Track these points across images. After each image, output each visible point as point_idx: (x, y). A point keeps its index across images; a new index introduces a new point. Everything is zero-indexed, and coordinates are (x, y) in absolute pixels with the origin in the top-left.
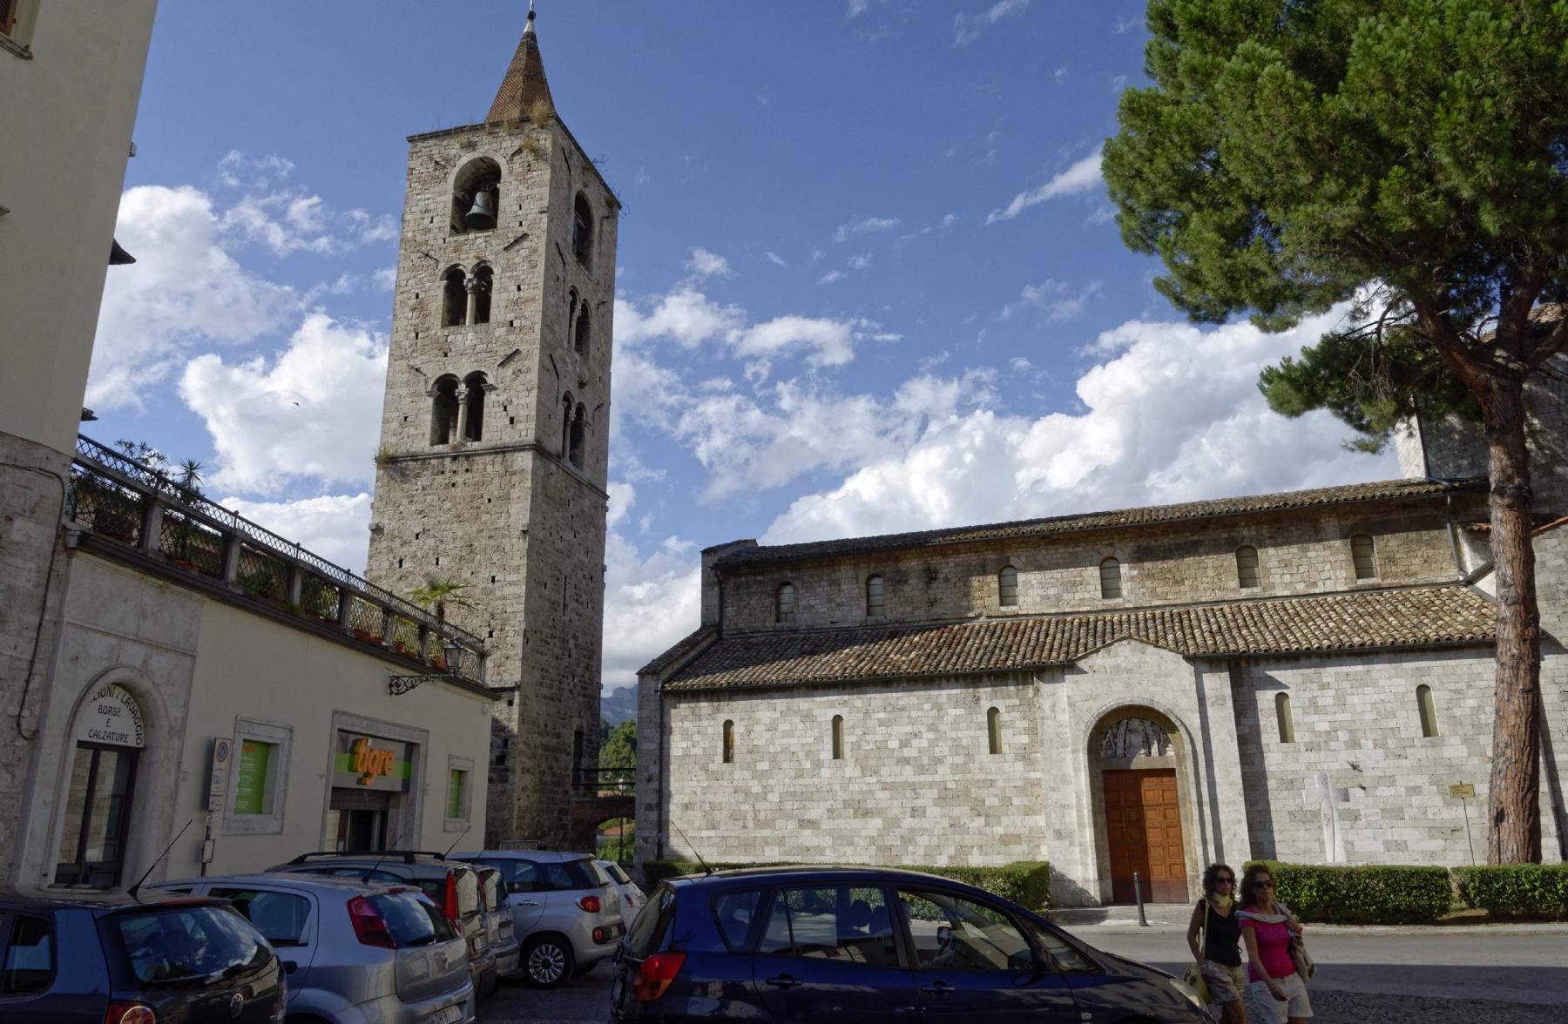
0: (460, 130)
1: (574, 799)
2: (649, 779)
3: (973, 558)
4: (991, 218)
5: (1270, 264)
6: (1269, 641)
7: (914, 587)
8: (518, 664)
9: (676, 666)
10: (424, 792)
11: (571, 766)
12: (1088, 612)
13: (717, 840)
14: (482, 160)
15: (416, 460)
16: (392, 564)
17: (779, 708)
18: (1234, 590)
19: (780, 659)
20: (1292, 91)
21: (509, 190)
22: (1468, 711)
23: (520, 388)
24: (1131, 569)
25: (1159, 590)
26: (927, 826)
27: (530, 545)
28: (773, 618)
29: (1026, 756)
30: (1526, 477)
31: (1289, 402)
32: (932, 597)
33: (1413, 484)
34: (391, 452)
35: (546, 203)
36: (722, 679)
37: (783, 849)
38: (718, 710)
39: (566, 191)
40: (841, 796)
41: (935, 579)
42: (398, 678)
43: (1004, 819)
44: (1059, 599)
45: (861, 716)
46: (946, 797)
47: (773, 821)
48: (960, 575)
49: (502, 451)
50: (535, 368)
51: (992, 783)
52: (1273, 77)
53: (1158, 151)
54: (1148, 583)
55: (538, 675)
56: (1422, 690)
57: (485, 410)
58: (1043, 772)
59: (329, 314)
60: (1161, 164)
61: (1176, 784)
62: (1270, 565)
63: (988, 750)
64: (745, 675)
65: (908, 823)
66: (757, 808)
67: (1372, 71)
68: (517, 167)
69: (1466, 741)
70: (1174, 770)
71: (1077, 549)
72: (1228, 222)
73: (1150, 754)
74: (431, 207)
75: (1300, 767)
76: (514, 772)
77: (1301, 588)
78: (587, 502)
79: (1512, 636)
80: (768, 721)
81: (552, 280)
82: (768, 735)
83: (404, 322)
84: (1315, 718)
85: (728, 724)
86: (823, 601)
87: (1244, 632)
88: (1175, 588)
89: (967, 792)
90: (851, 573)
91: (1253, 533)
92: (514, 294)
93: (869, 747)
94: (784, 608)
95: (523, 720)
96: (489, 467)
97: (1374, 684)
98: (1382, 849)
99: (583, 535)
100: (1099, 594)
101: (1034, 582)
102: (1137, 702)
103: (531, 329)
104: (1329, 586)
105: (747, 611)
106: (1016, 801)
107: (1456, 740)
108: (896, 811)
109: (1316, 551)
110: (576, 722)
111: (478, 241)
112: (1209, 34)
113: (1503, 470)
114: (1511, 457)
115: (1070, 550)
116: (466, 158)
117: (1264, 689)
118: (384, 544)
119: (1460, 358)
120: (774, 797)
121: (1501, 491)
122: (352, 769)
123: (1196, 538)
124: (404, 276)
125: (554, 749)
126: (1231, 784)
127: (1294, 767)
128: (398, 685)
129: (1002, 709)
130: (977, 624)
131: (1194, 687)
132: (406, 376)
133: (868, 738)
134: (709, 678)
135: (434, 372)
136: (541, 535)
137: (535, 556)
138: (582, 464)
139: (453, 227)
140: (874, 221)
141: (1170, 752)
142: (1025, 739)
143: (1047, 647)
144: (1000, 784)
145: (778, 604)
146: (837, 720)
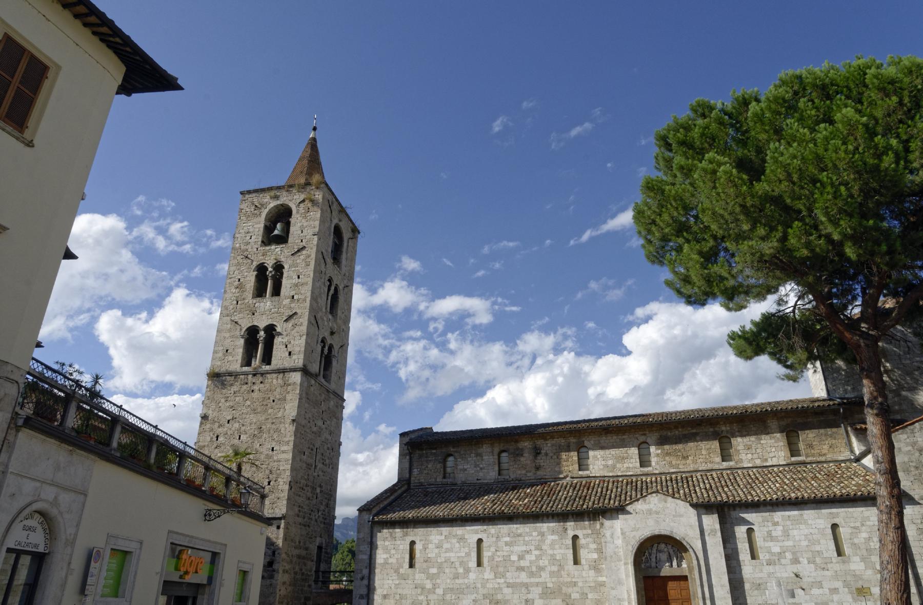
0: (270, 189)
1: (314, 591)
2: (362, 579)
3: (562, 441)
4: (572, 242)
5: (729, 273)
6: (741, 495)
7: (526, 459)
8: (285, 502)
9: (382, 506)
10: (221, 585)
11: (314, 569)
12: (631, 475)
14: (282, 205)
15: (231, 376)
16: (212, 438)
18: (718, 463)
19: (445, 502)
20: (736, 180)
21: (296, 222)
22: (863, 541)
23: (296, 334)
24: (656, 449)
25: (674, 463)
27: (296, 429)
28: (441, 476)
29: (595, 567)
30: (885, 397)
31: (745, 351)
32: (537, 464)
33: (821, 401)
34: (217, 370)
35: (317, 230)
36: (410, 514)
38: (406, 535)
40: (482, 591)
41: (539, 453)
42: (210, 510)
44: (614, 467)
45: (494, 539)
48: (555, 451)
49: (283, 371)
50: (306, 323)
51: (575, 584)
52: (725, 172)
53: (664, 210)
54: (667, 458)
55: (296, 509)
56: (834, 527)
57: (274, 347)
58: (607, 577)
59: (187, 288)
60: (666, 217)
61: (688, 585)
62: (739, 448)
64: (424, 512)
66: (429, 598)
67: (779, 170)
68: (301, 210)
69: (863, 559)
70: (686, 577)
71: (624, 437)
72: (705, 250)
73: (671, 566)
74: (251, 230)
75: (764, 575)
76: (278, 572)
77: (758, 462)
78: (332, 403)
79: (885, 494)
80: (437, 542)
81: (318, 272)
82: (437, 551)
83: (231, 295)
84: (771, 544)
85: (413, 543)
86: (472, 466)
87: (726, 489)
88: (684, 462)
90: (489, 450)
91: (728, 428)
92: (296, 280)
94: (449, 470)
95: (285, 539)
96: (275, 381)
97: (806, 523)
99: (328, 422)
100: (638, 464)
101: (599, 456)
102: (663, 532)
103: (305, 300)
104: (774, 462)
105: (425, 472)
106: (590, 596)
107: (857, 559)
109: (766, 440)
110: (318, 540)
111: (277, 250)
112: (689, 149)
113: (871, 393)
114: (875, 385)
116: (273, 204)
117: (739, 525)
118: (208, 426)
119: (841, 328)
120: (440, 591)
121: (871, 406)
122: (177, 569)
123: (694, 431)
124: (233, 268)
125: (304, 558)
126: (722, 586)
127: (760, 575)
128: (210, 515)
129: (581, 536)
130: (565, 482)
131: (697, 524)
132: (229, 326)
133: (498, 553)
134: (402, 514)
135: (246, 324)
136: (304, 422)
137: (299, 435)
138: (330, 380)
139: (263, 242)
140: (505, 243)
141: (684, 565)
142: (595, 556)
143: (608, 497)
144: (580, 584)
145: (445, 467)
146: (480, 541)
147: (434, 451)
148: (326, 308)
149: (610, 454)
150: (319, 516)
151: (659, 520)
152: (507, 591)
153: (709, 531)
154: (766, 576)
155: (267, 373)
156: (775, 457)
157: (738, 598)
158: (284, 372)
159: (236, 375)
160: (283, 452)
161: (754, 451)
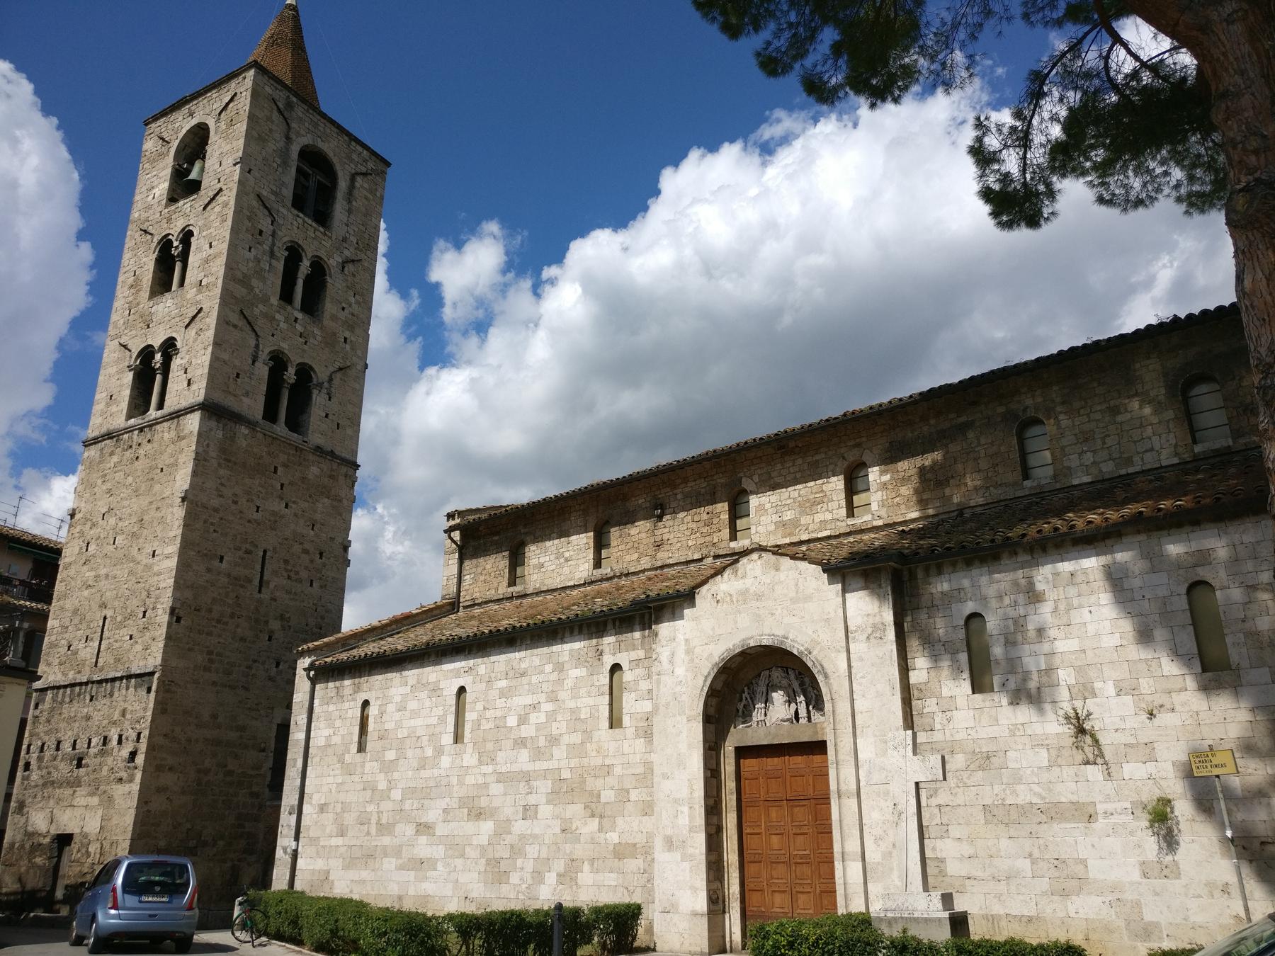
8: (161, 645)
13: (343, 850)
15: (112, 438)
16: (81, 548)
17: (411, 681)
24: (882, 473)
26: (537, 831)
35: (240, 154)
37: (400, 861)
38: (357, 689)
39: (281, 144)
40: (458, 792)
43: (620, 821)
44: (795, 523)
46: (563, 791)
47: (394, 824)
49: (177, 415)
51: (608, 770)
63: (607, 724)
65: (519, 827)
68: (223, 126)
71: (818, 457)
78: (314, 470)
80: (398, 699)
82: (397, 716)
85: (366, 704)
86: (552, 557)
89: (583, 780)
91: (1039, 400)
93: (487, 727)
96: (166, 434)
98: (1136, 875)
99: (305, 505)
100: (843, 512)
103: (215, 285)
104: (1150, 461)
105: (482, 578)
106: (634, 795)
108: (508, 811)
115: (809, 459)
120: (396, 794)
123: (963, 419)
127: (993, 731)
129: (625, 666)
133: (489, 714)
135: (136, 347)
142: (647, 706)
144: (618, 771)
146: (462, 690)
147: (496, 538)
148: (286, 296)
149: (789, 498)
150: (280, 673)
151: (762, 612)
152: (496, 789)
153: (870, 630)
154: (1007, 733)
155: (158, 423)
156: (1152, 449)
157: (936, 790)
158: (178, 417)
159: (118, 436)
160: (167, 558)
161: (1099, 442)
